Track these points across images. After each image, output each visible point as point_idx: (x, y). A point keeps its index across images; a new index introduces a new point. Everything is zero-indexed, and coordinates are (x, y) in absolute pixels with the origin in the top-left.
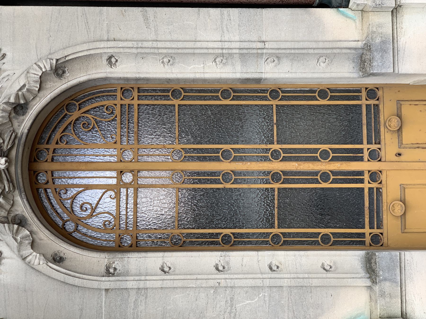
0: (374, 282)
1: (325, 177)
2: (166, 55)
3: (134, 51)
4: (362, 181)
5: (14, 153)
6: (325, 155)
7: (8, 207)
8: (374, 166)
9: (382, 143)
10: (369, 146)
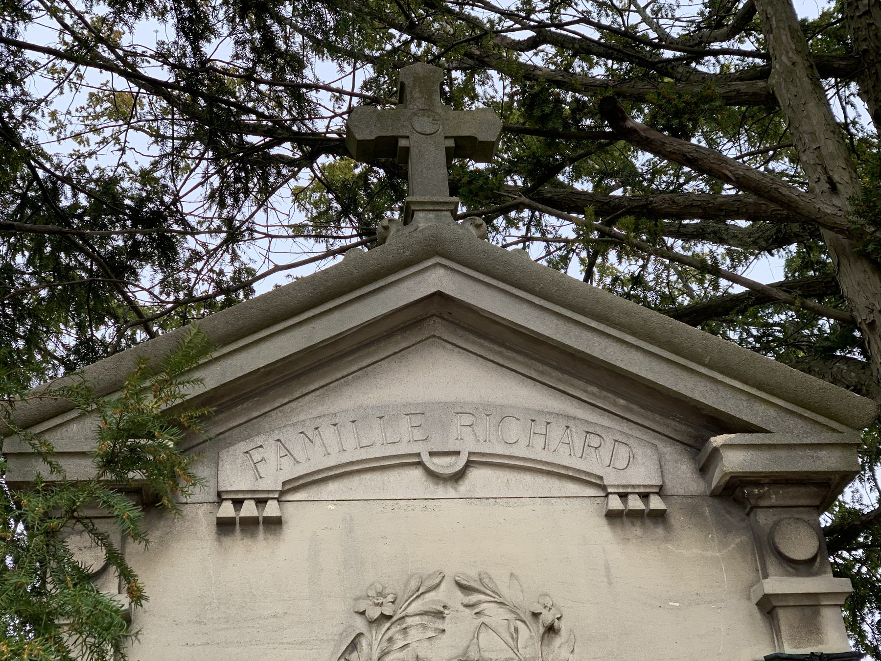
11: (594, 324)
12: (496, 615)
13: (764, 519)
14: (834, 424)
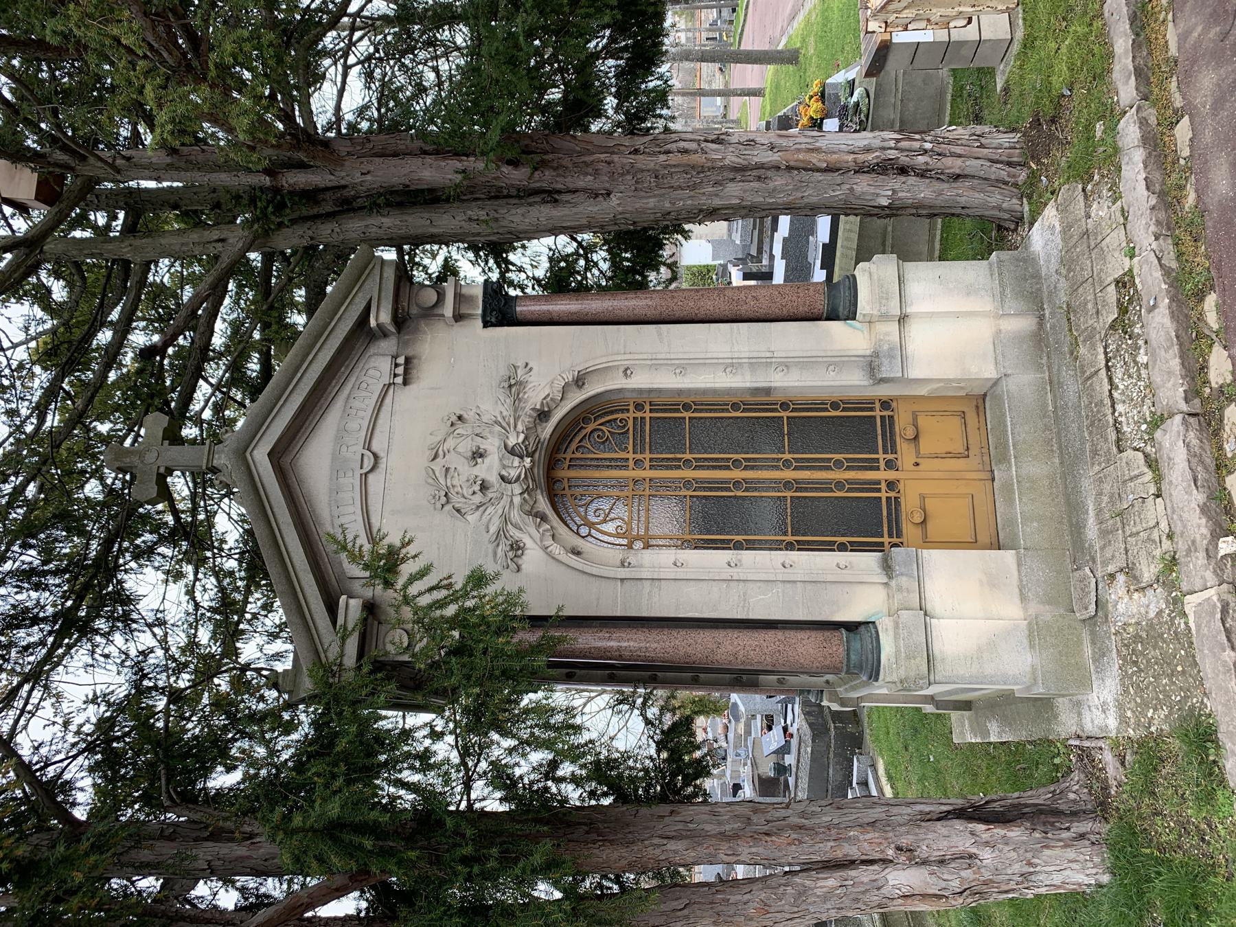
0: (890, 578)
1: (839, 485)
2: (678, 366)
3: (649, 362)
4: (879, 490)
5: (537, 455)
6: (839, 464)
7: (532, 503)
8: (891, 475)
9: (899, 452)
10: (885, 456)
11: (299, 375)
12: (450, 443)
14: (371, 266)
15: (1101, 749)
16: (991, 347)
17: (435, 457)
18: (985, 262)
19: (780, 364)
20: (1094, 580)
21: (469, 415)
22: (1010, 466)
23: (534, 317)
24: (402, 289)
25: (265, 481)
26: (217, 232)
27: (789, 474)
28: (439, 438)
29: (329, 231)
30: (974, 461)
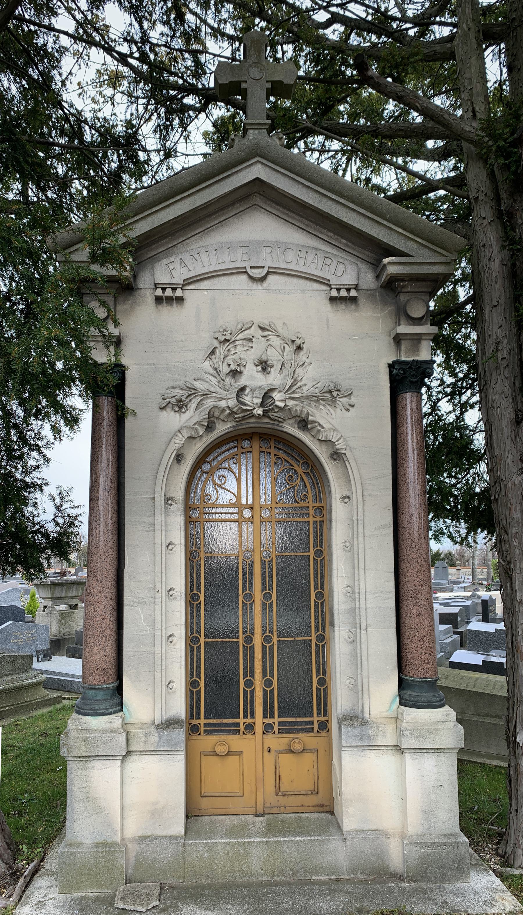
0: (158, 727)
1: (249, 684)
2: (352, 545)
3: (355, 518)
4: (245, 717)
5: (267, 420)
6: (268, 683)
8: (259, 728)
9: (280, 736)
10: (276, 723)
12: (275, 341)
13: (403, 298)
14: (444, 252)
15: (10, 897)
16: (373, 827)
17: (263, 329)
18: (457, 829)
19: (355, 636)
20: (144, 910)
21: (302, 356)
22: (260, 836)
23: (400, 411)
24: (424, 283)
25: (233, 178)
26: (483, 109)
27: (258, 640)
28: (280, 330)
29: (483, 216)
30: (272, 799)
